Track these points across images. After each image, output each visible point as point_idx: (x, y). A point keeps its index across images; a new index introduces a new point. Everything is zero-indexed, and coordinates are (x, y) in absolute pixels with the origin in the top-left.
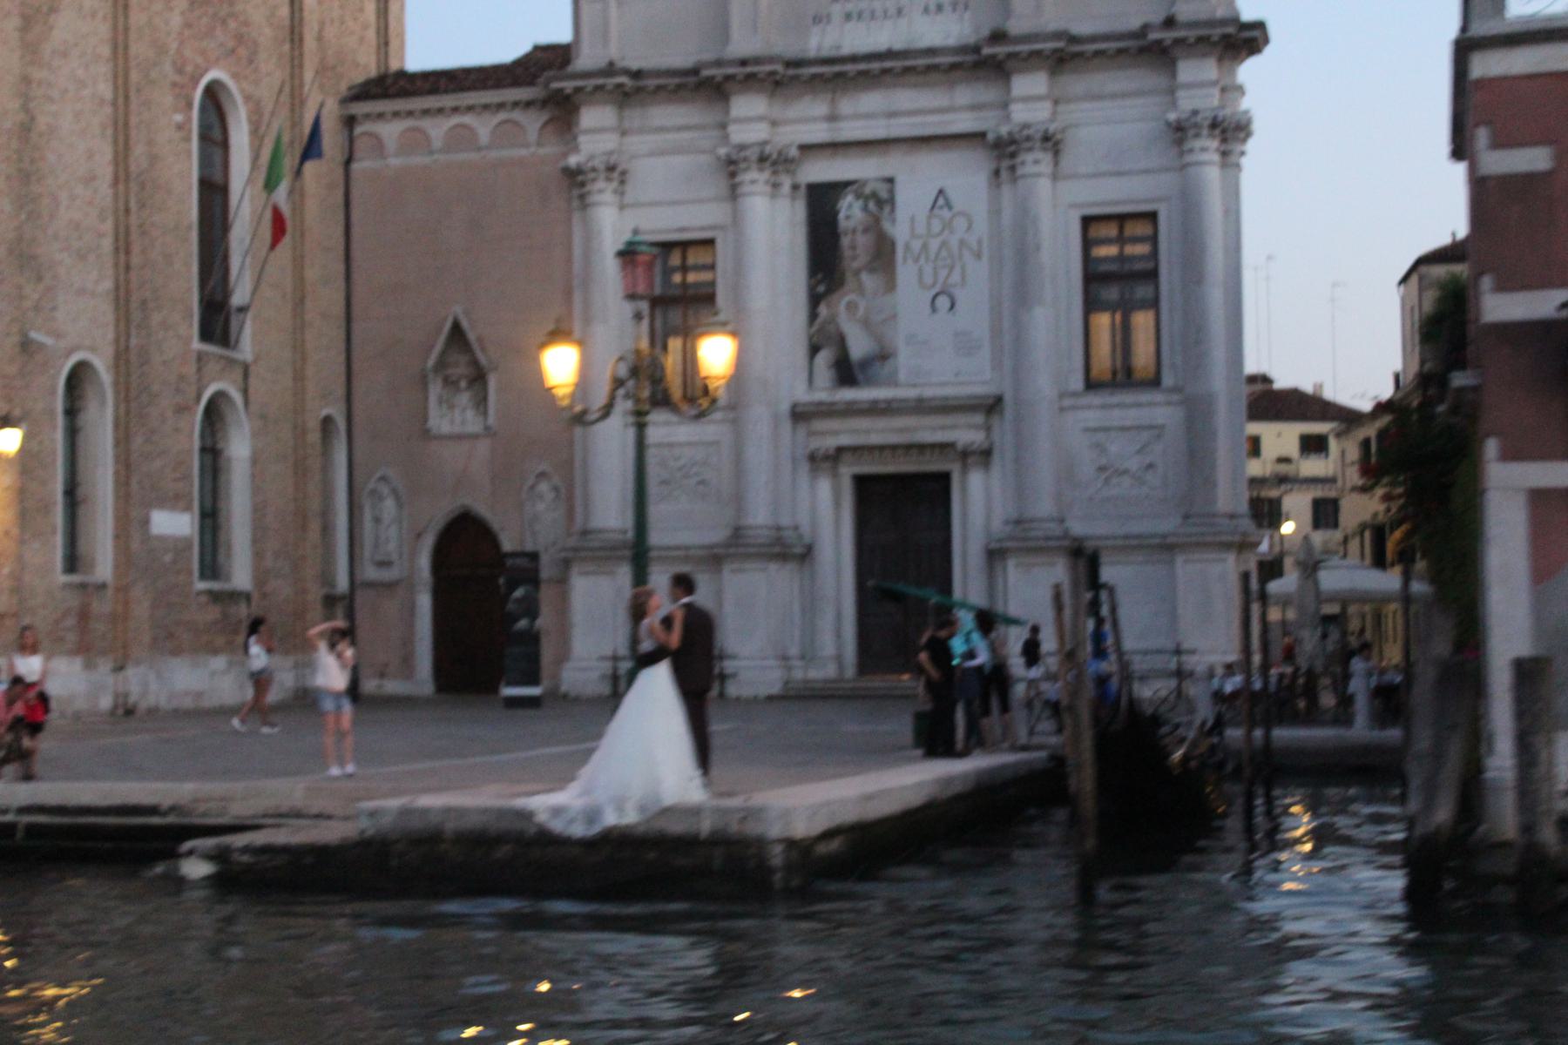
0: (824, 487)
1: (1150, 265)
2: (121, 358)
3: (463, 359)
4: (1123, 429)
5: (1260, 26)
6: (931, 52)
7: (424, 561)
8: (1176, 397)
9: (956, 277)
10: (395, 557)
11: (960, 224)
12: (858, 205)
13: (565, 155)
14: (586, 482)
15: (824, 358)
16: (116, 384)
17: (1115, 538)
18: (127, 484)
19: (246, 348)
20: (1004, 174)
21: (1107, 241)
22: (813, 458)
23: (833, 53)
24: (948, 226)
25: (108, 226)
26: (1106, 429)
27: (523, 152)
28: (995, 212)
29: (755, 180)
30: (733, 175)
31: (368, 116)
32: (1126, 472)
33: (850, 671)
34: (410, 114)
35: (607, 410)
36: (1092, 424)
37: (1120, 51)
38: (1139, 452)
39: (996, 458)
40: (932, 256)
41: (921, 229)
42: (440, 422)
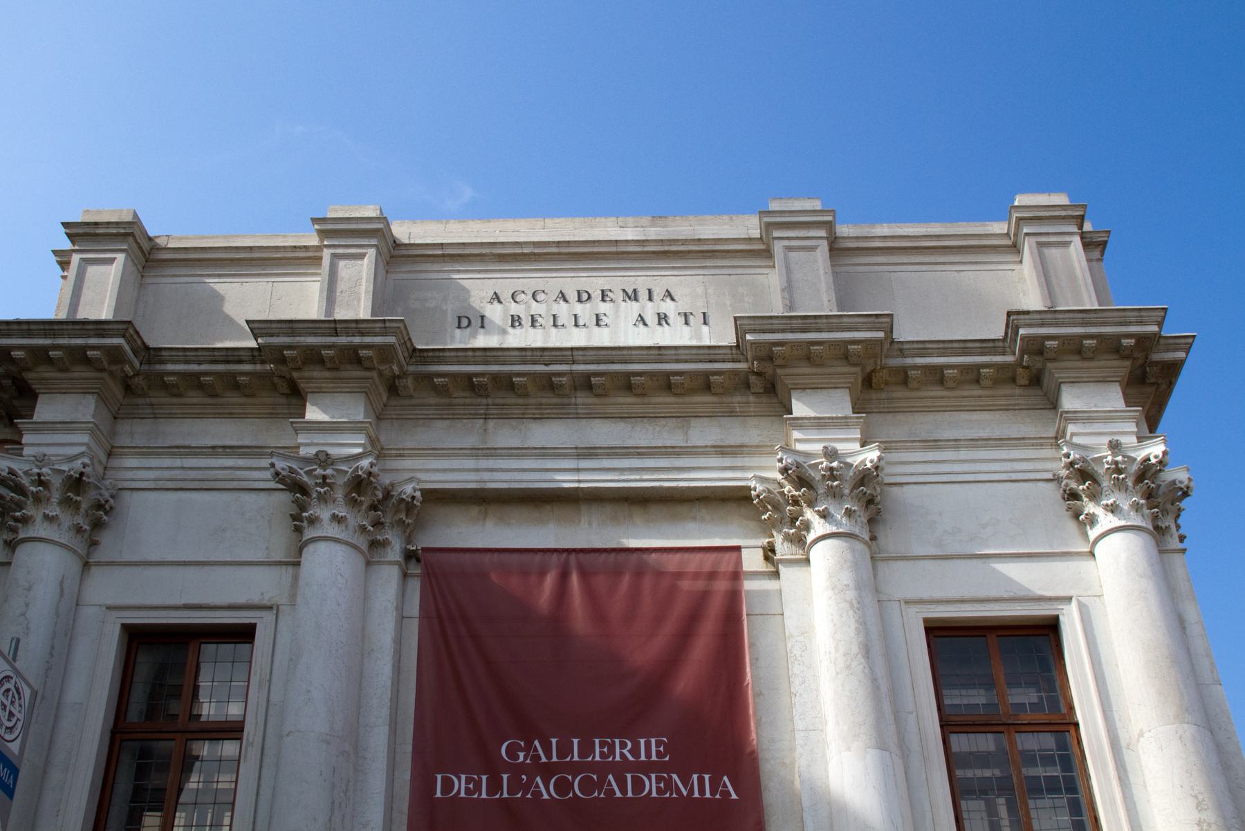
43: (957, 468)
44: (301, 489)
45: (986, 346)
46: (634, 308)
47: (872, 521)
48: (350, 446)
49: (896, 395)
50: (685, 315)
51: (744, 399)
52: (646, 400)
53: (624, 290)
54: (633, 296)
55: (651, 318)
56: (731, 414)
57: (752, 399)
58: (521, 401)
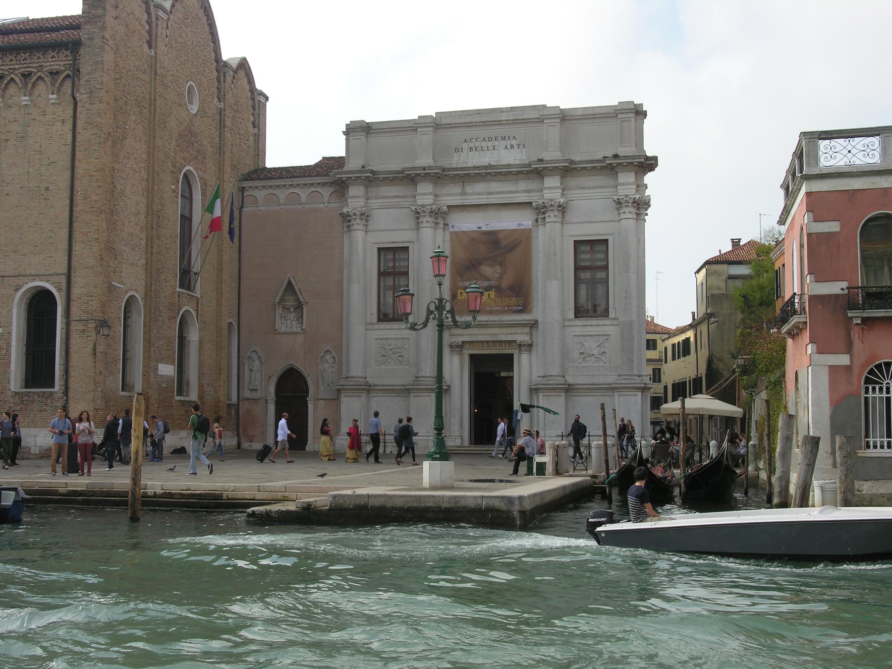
0: (456, 359)
1: (605, 263)
2: (146, 297)
3: (292, 298)
4: (591, 336)
5: (655, 159)
6: (509, 166)
7: (272, 389)
8: (615, 323)
10: (258, 388)
13: (342, 208)
14: (348, 356)
16: (145, 306)
17: (588, 385)
18: (149, 351)
19: (198, 293)
20: (539, 220)
21: (586, 252)
22: (451, 346)
23: (465, 166)
25: (144, 235)
26: (584, 336)
27: (322, 206)
29: (426, 220)
30: (418, 218)
31: (250, 187)
33: (466, 443)
34: (270, 187)
35: (425, 324)
36: (578, 334)
38: (598, 346)
39: (534, 349)
42: (281, 326)
43: (589, 195)
44: (418, 213)
45: (598, 161)
46: (504, 143)
47: (563, 215)
48: (428, 200)
54: (504, 139)
55: (509, 147)
56: (530, 179)
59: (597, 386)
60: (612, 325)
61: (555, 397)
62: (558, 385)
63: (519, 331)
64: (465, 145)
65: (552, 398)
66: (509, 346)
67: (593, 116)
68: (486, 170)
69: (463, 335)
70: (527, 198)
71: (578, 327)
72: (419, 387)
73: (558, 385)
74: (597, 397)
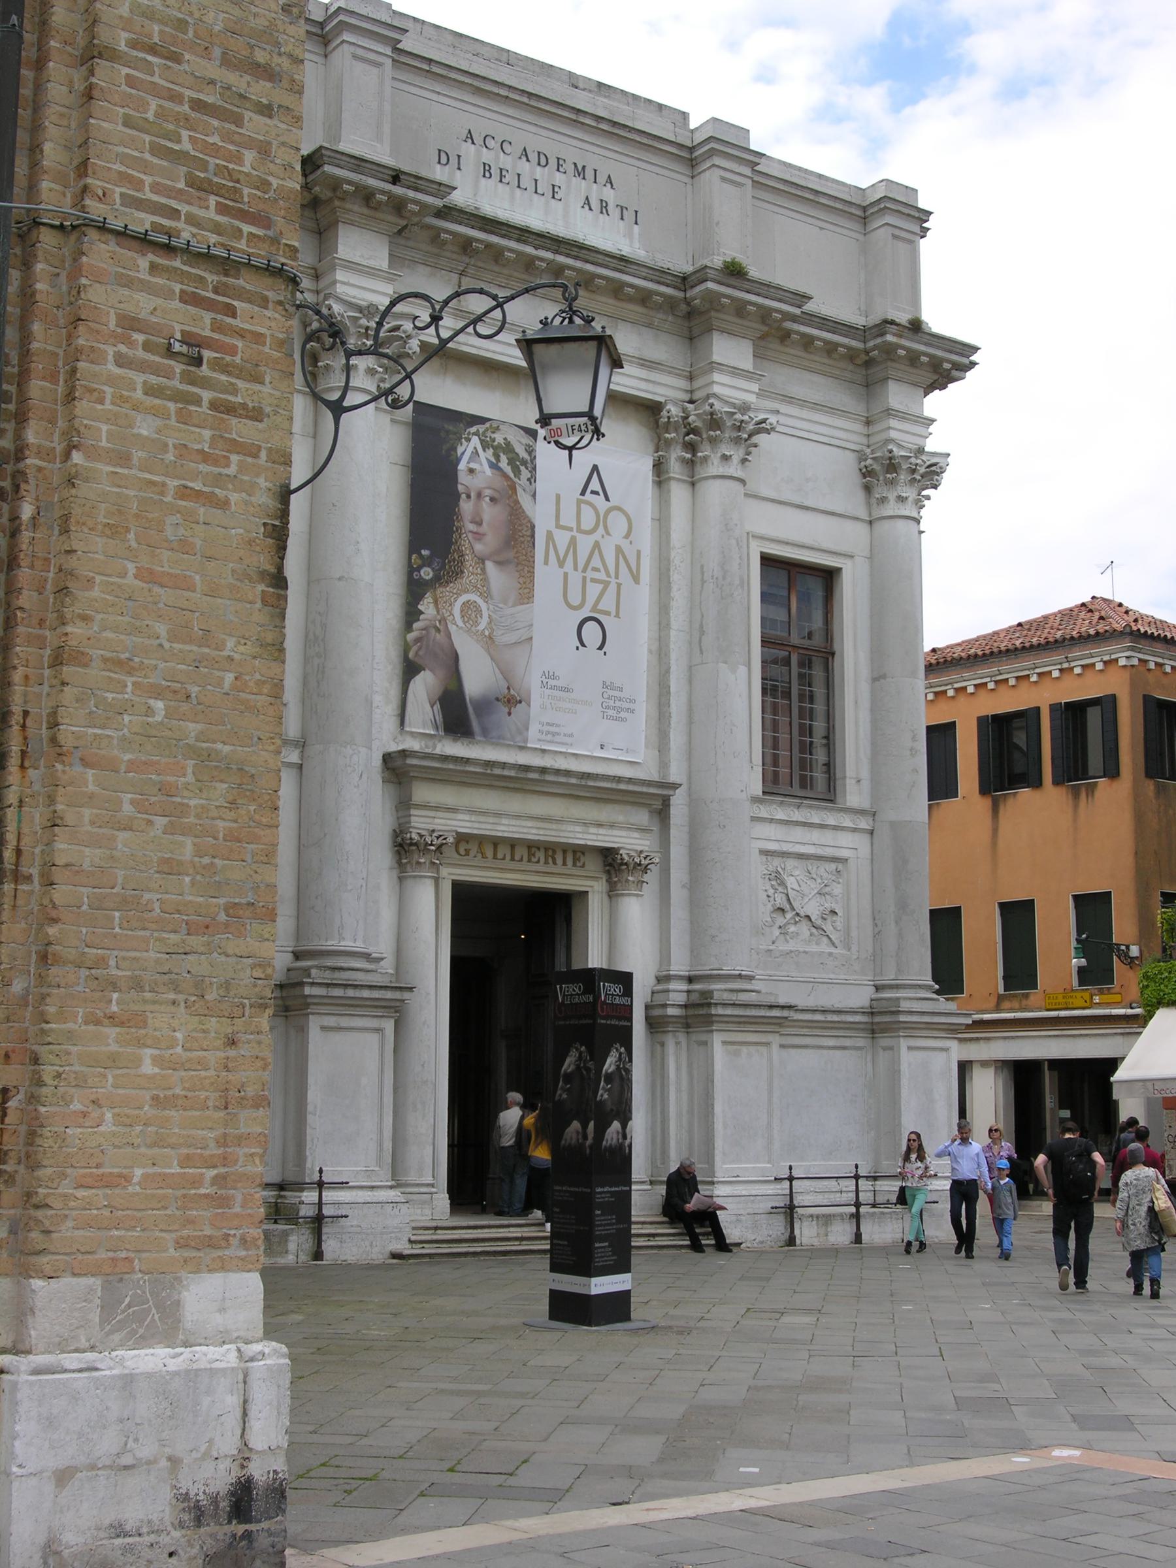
4: (801, 856)
6: (622, 262)
8: (864, 823)
9: (608, 603)
11: (618, 524)
12: (486, 456)
15: (424, 685)
17: (814, 1011)
20: (675, 468)
24: (602, 521)
26: (783, 855)
28: (662, 521)
32: (808, 917)
37: (831, 349)
40: (581, 565)
41: (568, 519)
43: (799, 424)
46: (581, 187)
49: (771, 346)
50: (622, 207)
51: (664, 317)
52: (593, 296)
53: (575, 164)
54: (581, 172)
55: (595, 204)
56: (649, 326)
57: (670, 318)
58: (496, 269)
59: (835, 1018)
60: (855, 830)
61: (752, 1049)
62: (771, 1007)
63: (621, 818)
64: (468, 150)
65: (745, 1050)
66: (574, 865)
67: (811, 197)
68: (557, 252)
69: (454, 810)
70: (643, 385)
71: (773, 826)
72: (351, 993)
73: (771, 1007)
74: (825, 1052)
